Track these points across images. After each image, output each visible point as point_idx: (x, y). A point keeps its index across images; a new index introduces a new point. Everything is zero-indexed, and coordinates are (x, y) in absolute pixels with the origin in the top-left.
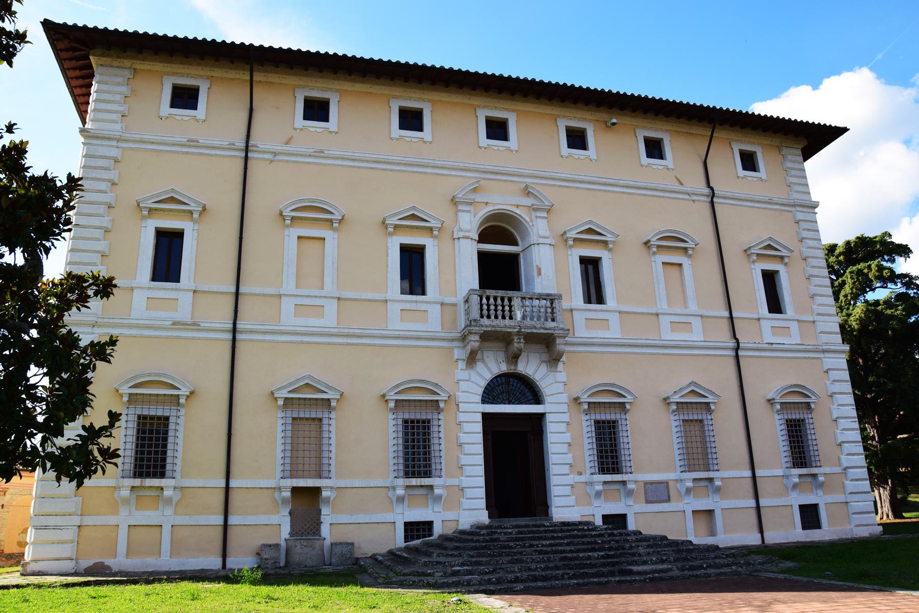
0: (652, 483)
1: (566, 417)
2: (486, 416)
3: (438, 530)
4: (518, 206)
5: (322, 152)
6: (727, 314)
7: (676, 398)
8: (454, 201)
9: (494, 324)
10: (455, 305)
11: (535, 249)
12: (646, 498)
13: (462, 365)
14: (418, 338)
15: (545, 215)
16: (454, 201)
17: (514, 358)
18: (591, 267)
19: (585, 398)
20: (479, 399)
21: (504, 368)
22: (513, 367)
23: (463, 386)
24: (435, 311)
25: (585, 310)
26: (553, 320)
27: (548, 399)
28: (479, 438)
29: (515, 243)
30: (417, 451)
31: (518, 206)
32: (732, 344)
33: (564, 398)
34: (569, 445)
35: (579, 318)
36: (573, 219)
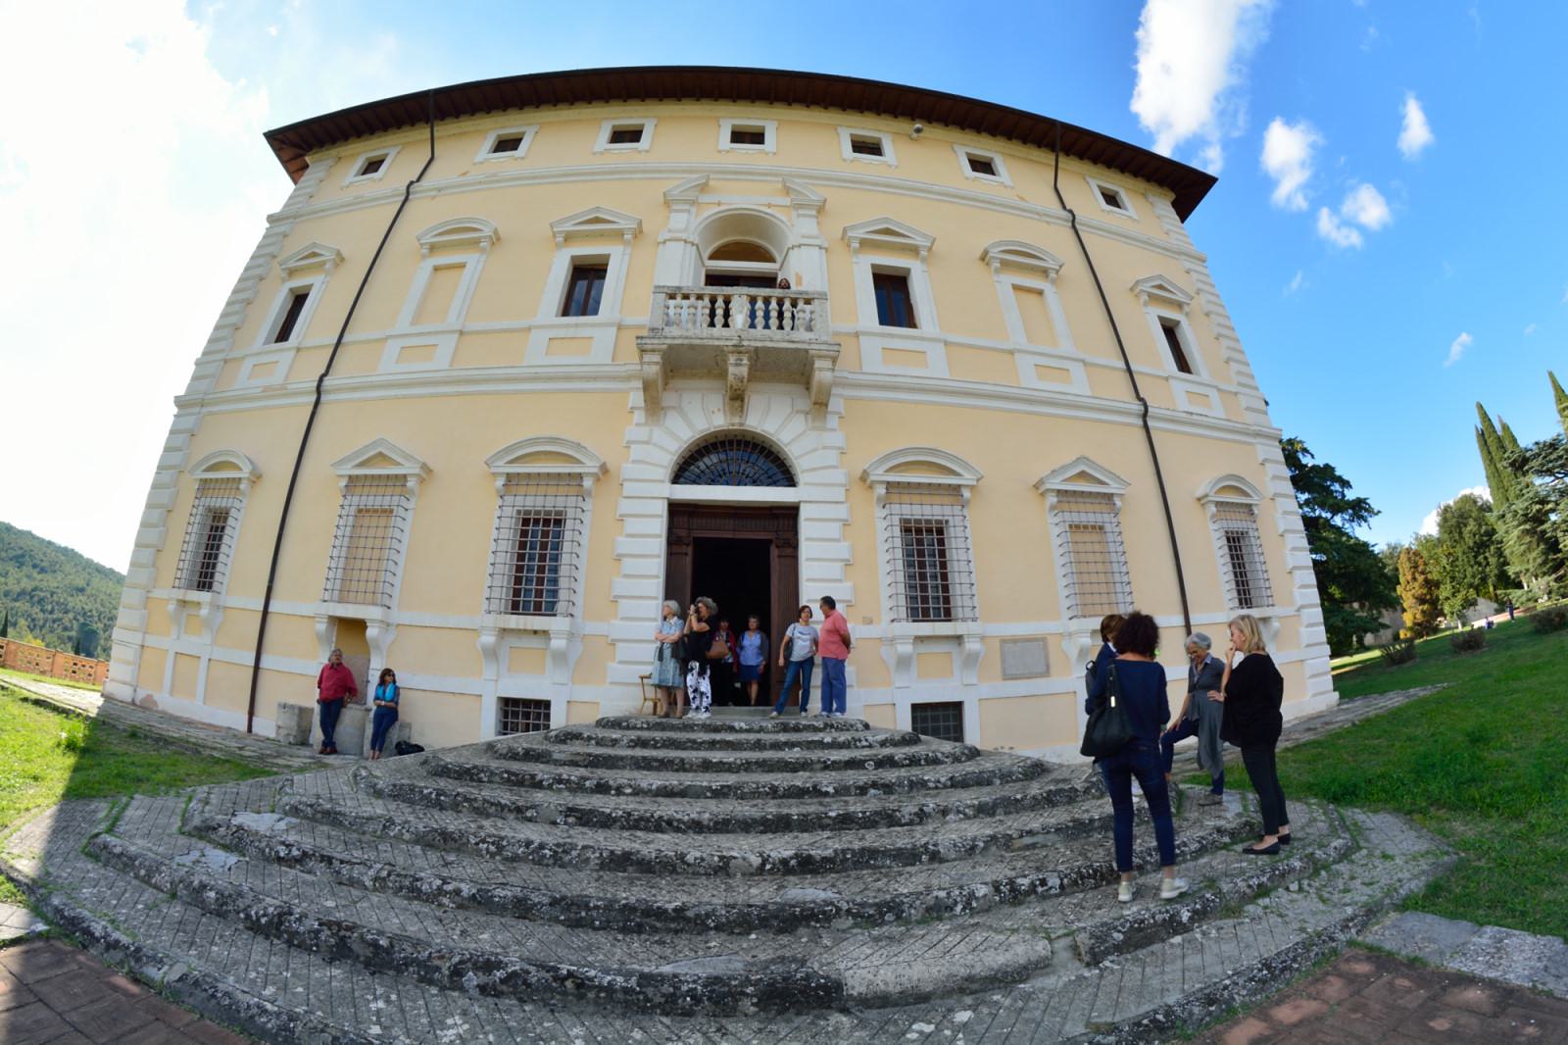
0: (1015, 641)
1: (842, 512)
2: (676, 509)
3: (558, 720)
4: (769, 206)
5: (495, 175)
6: (1122, 365)
7: (1057, 484)
9: (690, 334)
12: (1004, 670)
13: (639, 416)
14: (569, 378)
17: (737, 399)
19: (879, 474)
20: (665, 472)
22: (736, 420)
23: (636, 451)
25: (882, 335)
26: (809, 329)
27: (801, 477)
28: (658, 546)
29: (771, 259)
30: (535, 567)
31: (769, 206)
32: (1138, 408)
33: (838, 476)
34: (848, 564)
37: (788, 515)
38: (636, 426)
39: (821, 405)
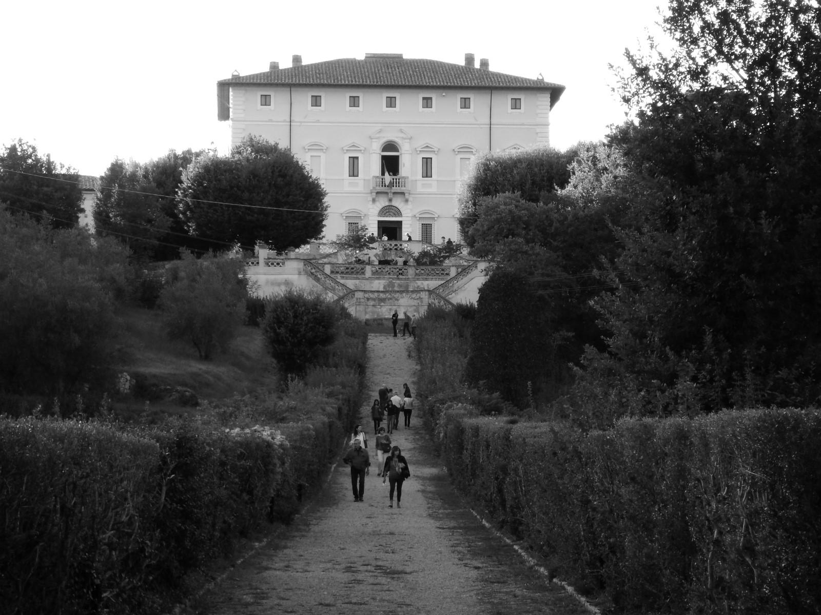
1: (410, 222)
2: (379, 222)
4: (397, 137)
8: (371, 138)
10: (369, 180)
11: (403, 155)
13: (371, 203)
15: (408, 141)
16: (371, 138)
17: (390, 200)
18: (427, 162)
21: (387, 204)
24: (361, 183)
26: (405, 186)
31: (397, 137)
35: (419, 184)
36: (419, 144)
37: (400, 223)
38: (370, 205)
39: (407, 201)
